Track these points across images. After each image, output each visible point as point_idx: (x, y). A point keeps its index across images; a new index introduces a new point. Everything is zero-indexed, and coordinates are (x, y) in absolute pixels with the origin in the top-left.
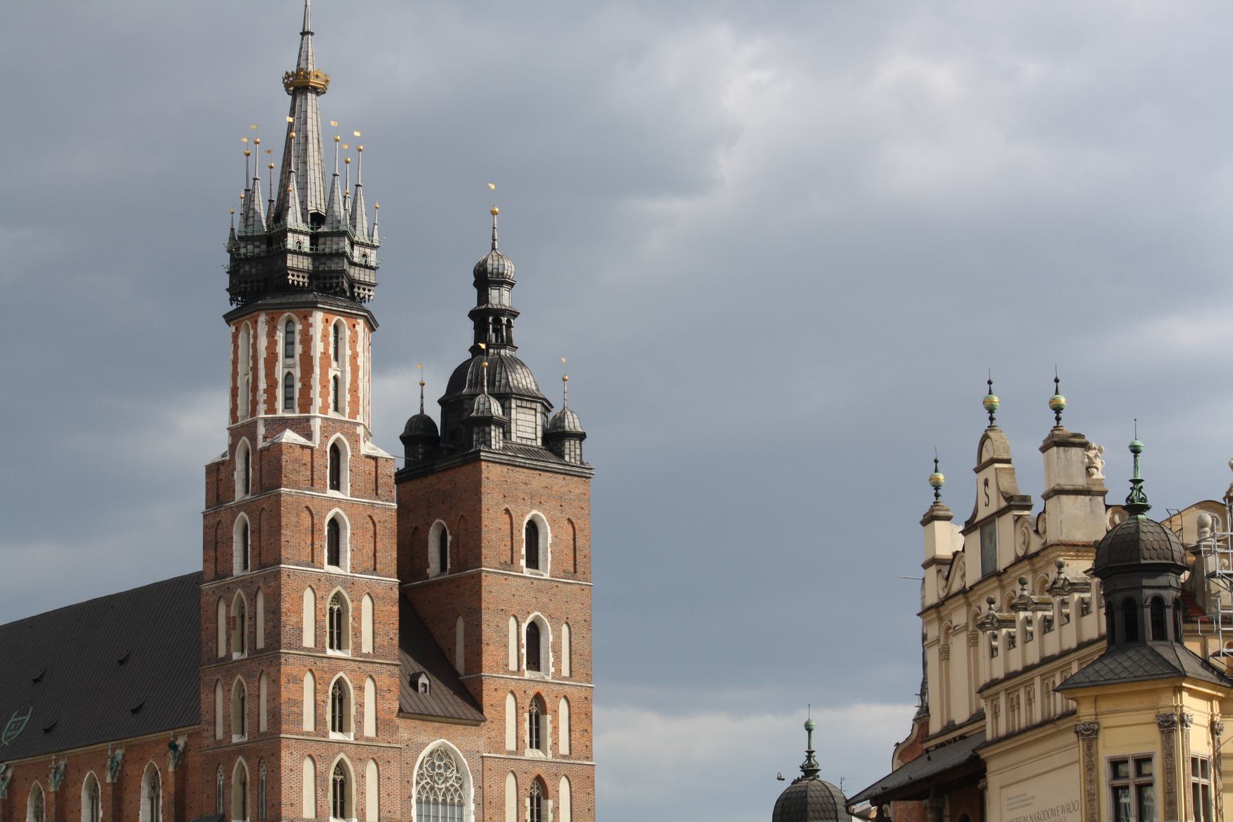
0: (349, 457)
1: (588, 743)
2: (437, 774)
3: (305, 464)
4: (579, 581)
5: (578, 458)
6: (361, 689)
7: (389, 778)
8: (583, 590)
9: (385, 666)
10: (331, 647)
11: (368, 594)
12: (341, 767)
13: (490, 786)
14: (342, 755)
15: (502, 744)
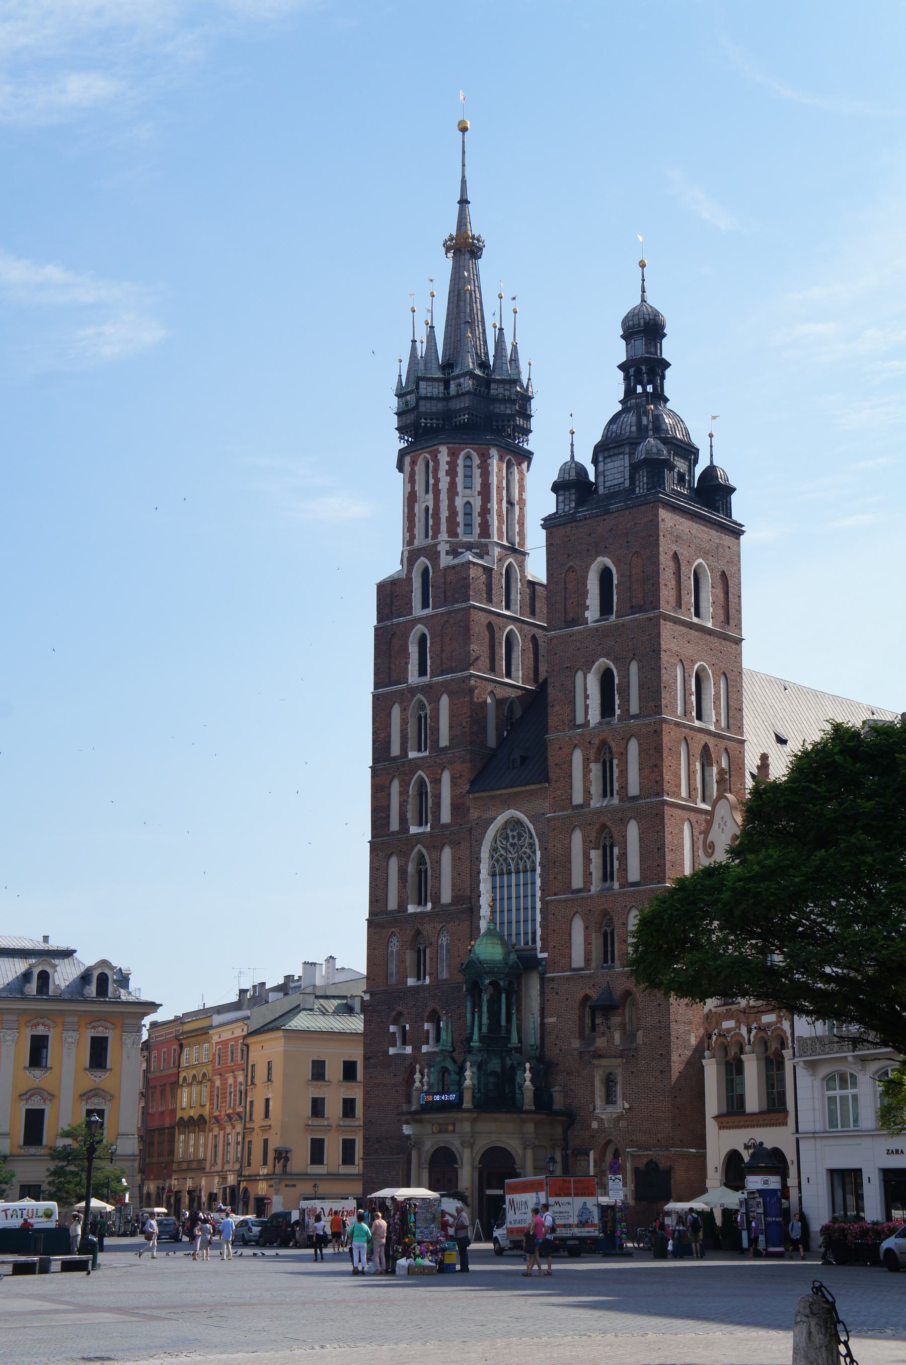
0: (431, 574)
1: (658, 778)
2: (513, 845)
3: (397, 596)
4: (648, 611)
5: (645, 487)
6: (437, 782)
7: (459, 859)
8: (651, 620)
9: (457, 754)
10: (419, 750)
11: (443, 692)
12: (421, 860)
13: (554, 846)
14: (419, 846)
15: (568, 801)
